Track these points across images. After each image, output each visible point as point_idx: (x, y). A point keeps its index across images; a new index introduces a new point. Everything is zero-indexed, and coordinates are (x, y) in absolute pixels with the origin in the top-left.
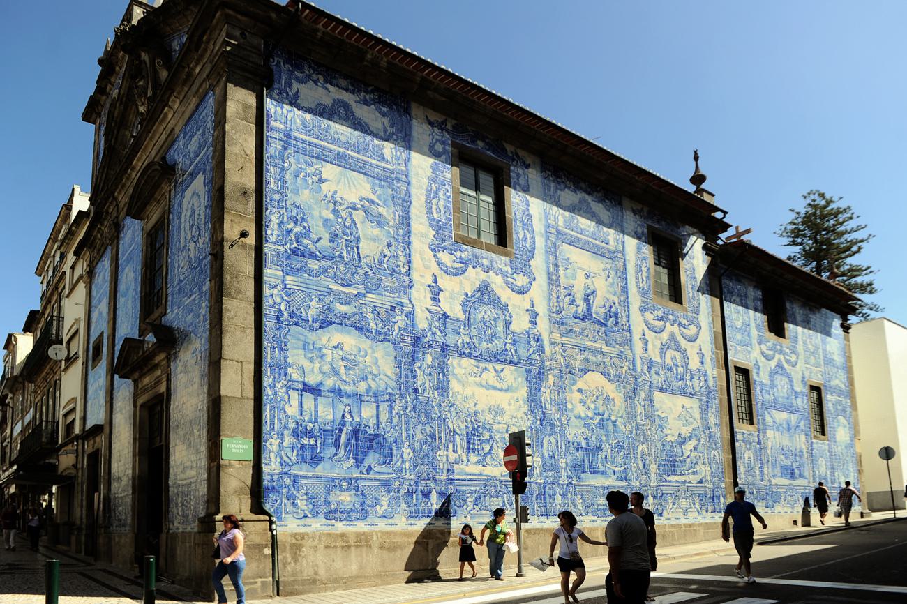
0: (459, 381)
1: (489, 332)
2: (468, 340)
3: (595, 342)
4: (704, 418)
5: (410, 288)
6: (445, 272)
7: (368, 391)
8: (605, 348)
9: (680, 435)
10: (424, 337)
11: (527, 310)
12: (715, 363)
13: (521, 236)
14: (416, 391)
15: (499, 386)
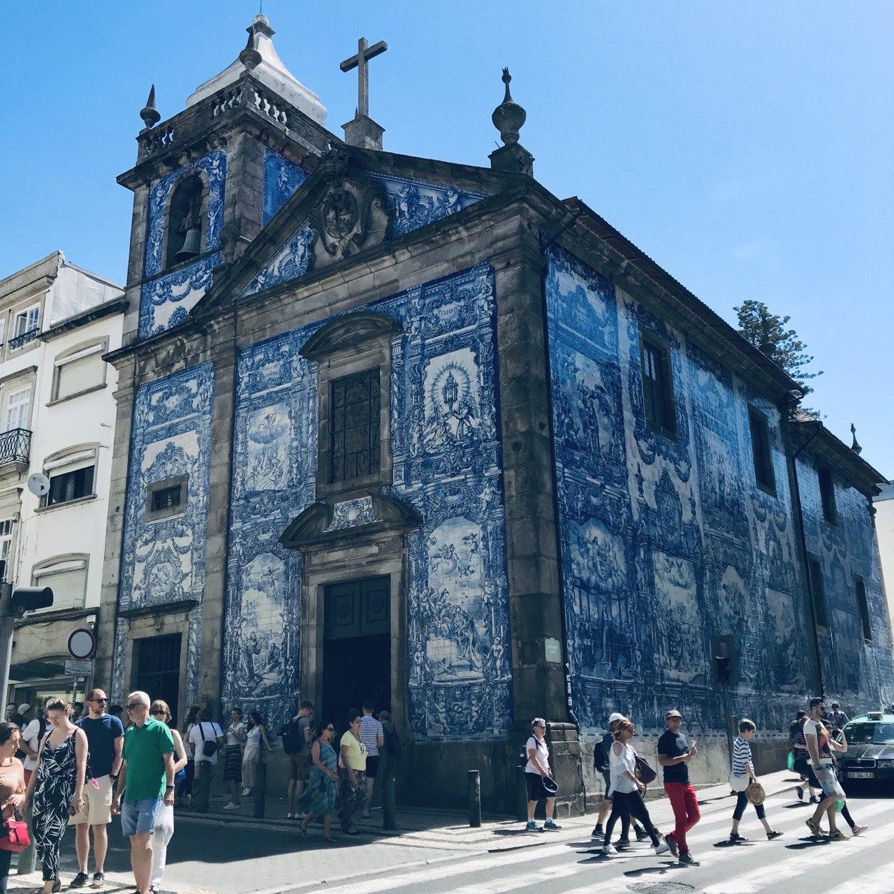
0: (660, 577)
1: (671, 524)
2: (661, 533)
3: (728, 533)
4: (797, 619)
5: (627, 476)
6: (645, 461)
7: (613, 585)
8: (736, 540)
9: (784, 637)
10: (639, 529)
11: (690, 499)
12: (799, 558)
13: (680, 420)
14: (638, 589)
15: (681, 581)
